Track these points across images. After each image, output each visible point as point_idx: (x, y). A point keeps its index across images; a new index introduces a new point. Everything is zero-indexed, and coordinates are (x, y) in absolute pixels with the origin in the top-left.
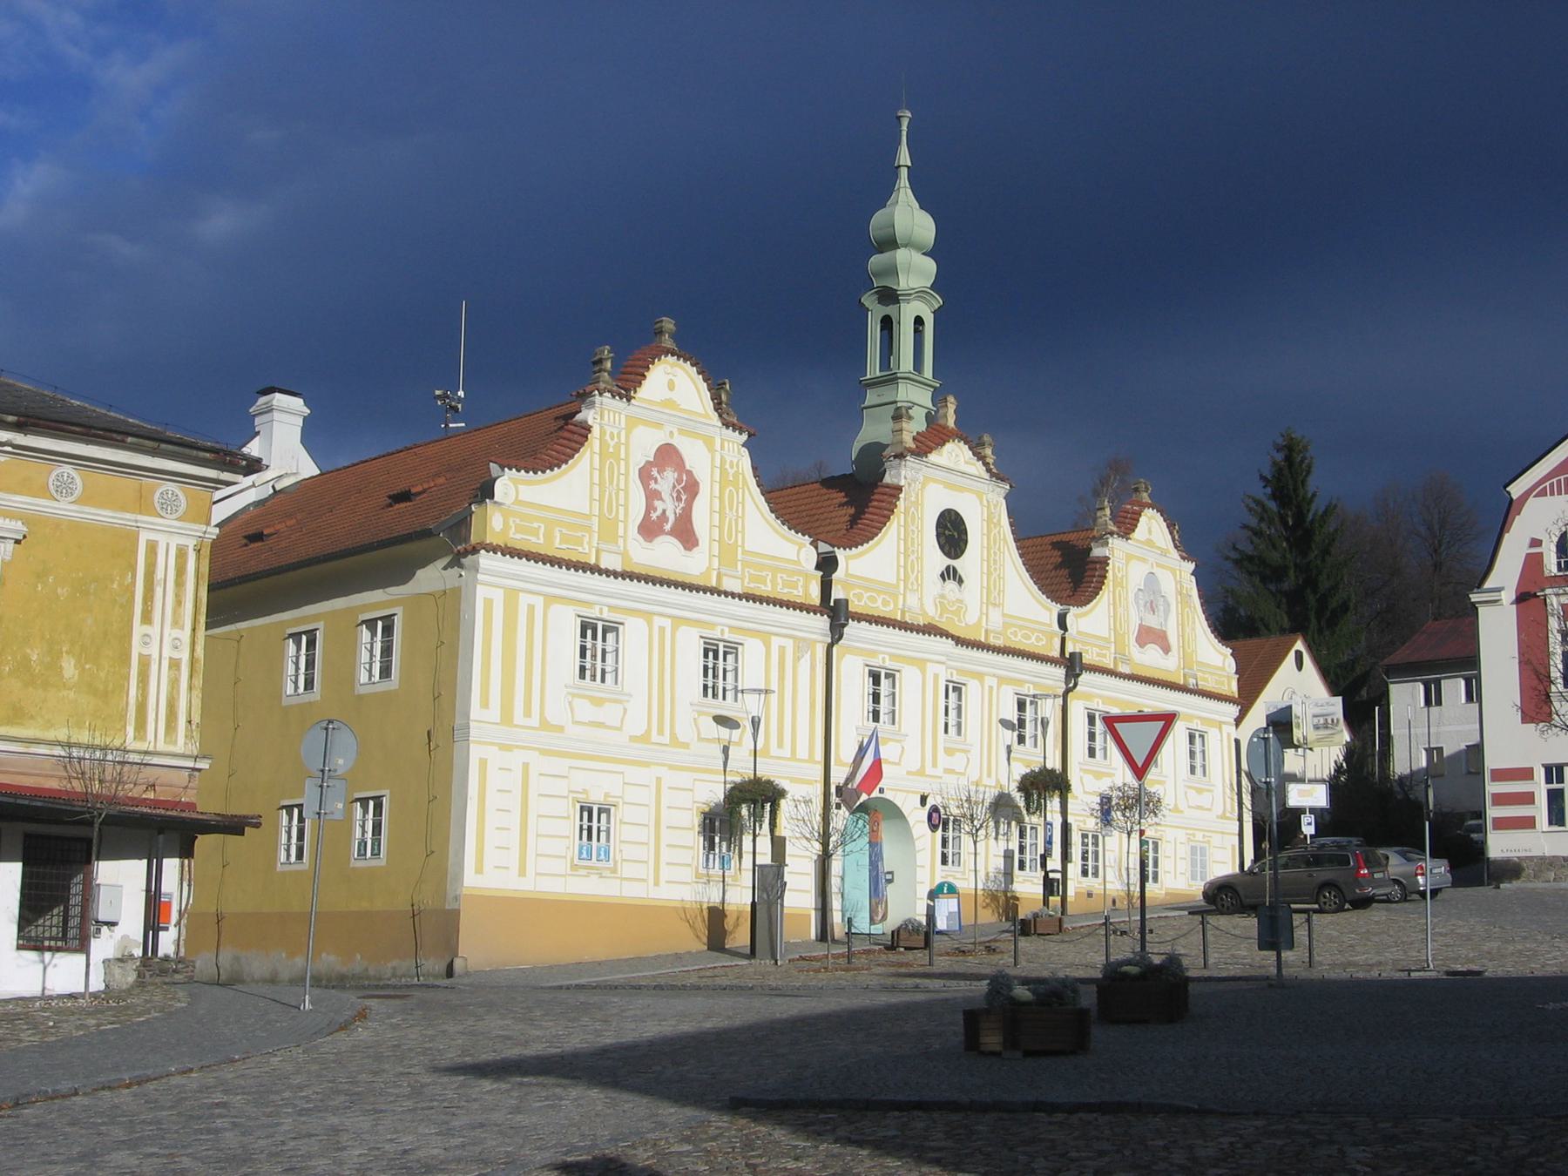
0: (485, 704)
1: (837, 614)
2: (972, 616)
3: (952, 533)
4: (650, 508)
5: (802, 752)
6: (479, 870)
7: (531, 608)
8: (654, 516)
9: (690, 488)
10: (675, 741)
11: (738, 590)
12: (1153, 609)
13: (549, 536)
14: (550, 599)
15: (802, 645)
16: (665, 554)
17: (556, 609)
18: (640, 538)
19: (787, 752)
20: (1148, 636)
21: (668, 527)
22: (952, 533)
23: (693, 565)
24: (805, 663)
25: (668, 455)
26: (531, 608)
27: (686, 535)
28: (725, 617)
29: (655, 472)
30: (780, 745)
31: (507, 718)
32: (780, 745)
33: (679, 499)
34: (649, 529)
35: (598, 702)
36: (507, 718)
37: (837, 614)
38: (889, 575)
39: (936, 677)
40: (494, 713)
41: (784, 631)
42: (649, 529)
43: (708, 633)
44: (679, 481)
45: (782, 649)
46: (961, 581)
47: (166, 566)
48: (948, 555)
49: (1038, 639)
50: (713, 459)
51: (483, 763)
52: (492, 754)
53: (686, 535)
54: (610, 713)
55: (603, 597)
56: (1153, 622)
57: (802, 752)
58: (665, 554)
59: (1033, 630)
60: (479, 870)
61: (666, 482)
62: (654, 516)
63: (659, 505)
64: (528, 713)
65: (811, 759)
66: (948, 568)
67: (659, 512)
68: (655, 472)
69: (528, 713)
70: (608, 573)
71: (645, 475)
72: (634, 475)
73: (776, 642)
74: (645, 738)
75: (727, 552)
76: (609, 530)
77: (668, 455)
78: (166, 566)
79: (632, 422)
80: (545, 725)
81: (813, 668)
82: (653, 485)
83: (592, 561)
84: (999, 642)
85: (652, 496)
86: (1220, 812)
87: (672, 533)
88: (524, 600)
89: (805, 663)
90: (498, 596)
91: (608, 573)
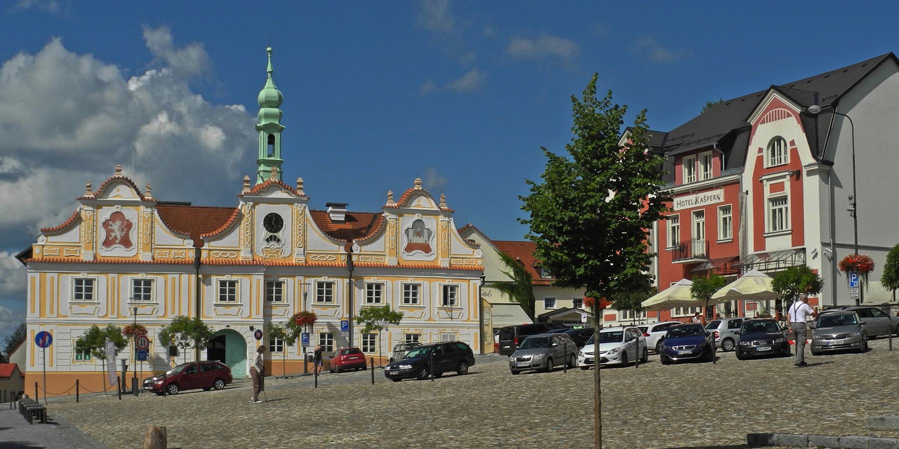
1: (198, 264)
9: (129, 225)
12: (419, 234)
25: (116, 216)
27: (126, 242)
29: (111, 223)
33: (123, 230)
34: (107, 243)
42: (107, 243)
46: (279, 241)
48: (271, 231)
53: (126, 242)
58: (118, 252)
61: (116, 226)
63: (113, 234)
68: (111, 223)
72: (100, 225)
87: (120, 243)
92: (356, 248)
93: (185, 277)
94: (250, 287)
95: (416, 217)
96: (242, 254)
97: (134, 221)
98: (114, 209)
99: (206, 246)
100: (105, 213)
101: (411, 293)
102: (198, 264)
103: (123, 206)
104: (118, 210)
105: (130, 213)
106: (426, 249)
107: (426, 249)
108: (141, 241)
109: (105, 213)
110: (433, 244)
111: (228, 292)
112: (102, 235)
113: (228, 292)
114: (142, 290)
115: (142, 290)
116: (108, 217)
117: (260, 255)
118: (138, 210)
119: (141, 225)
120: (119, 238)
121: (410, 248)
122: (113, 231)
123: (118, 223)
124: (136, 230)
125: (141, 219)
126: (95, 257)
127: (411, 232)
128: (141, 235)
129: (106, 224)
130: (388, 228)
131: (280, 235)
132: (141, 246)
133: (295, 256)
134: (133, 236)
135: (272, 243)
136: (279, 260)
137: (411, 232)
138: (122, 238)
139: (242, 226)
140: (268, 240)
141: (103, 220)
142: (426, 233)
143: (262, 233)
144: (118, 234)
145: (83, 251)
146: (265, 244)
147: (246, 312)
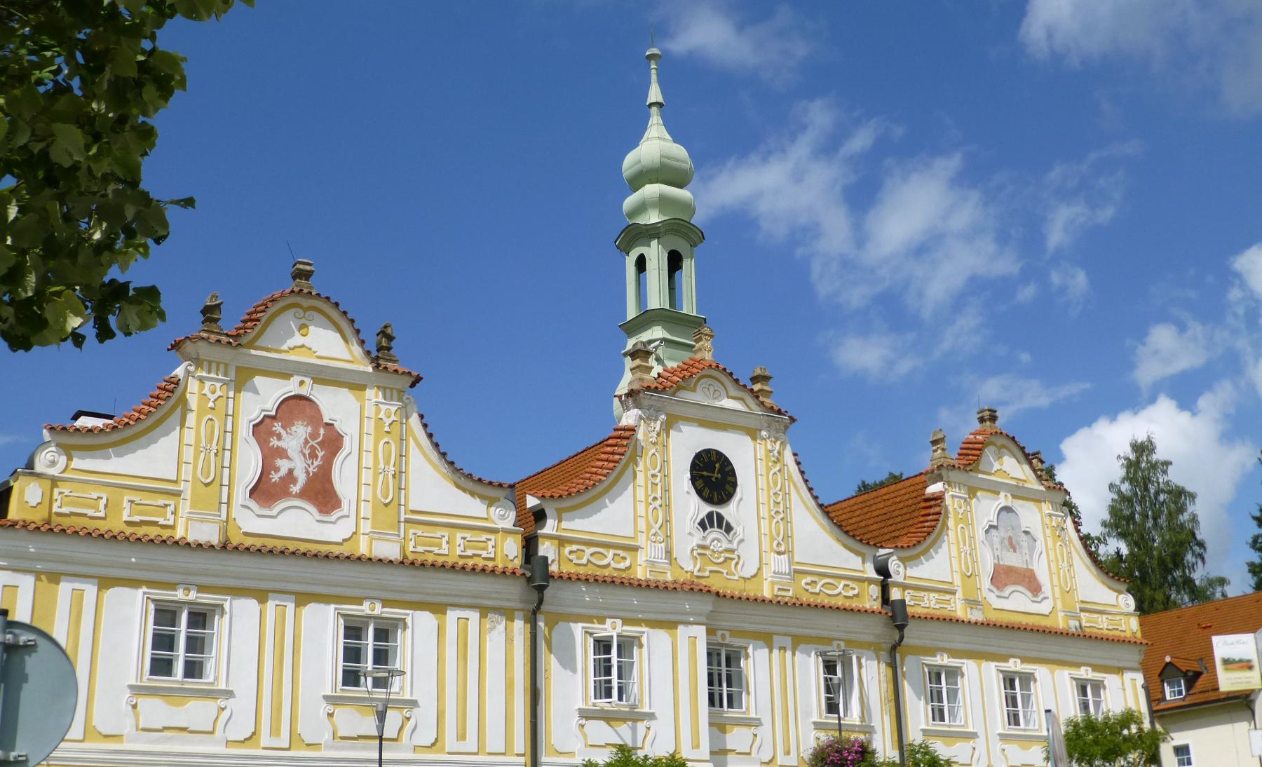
1: (535, 577)
3: (713, 478)
8: (275, 477)
9: (332, 442)
10: (295, 739)
12: (1012, 546)
18: (252, 504)
20: (1003, 577)
21: (296, 489)
22: (713, 478)
25: (296, 406)
27: (322, 494)
29: (278, 427)
33: (313, 456)
34: (265, 491)
41: (464, 601)
42: (265, 491)
44: (314, 436)
46: (729, 529)
48: (708, 500)
50: (362, 409)
53: (322, 494)
54: (196, 712)
56: (1012, 560)
58: (295, 522)
61: (294, 439)
62: (275, 477)
63: (284, 465)
66: (710, 515)
67: (283, 472)
71: (262, 429)
72: (245, 430)
81: (509, 640)
82: (274, 442)
83: (179, 533)
85: (271, 456)
87: (303, 495)
95: (1004, 500)
96: (642, 557)
97: (348, 427)
98: (291, 387)
99: (550, 527)
100: (268, 394)
103: (316, 381)
104: (304, 391)
105: (336, 405)
107: (1030, 582)
108: (366, 493)
109: (268, 394)
112: (249, 463)
116: (271, 406)
117: (689, 566)
118: (361, 400)
119: (368, 443)
120: (302, 478)
122: (282, 453)
123: (301, 430)
124: (354, 458)
125: (369, 426)
126: (224, 530)
128: (367, 476)
129: (262, 429)
130: (951, 523)
131: (728, 512)
132: (366, 510)
133: (767, 573)
134: (344, 478)
135: (714, 533)
139: (641, 478)
140: (702, 524)
144: (297, 465)
145: (185, 508)
146: (698, 537)
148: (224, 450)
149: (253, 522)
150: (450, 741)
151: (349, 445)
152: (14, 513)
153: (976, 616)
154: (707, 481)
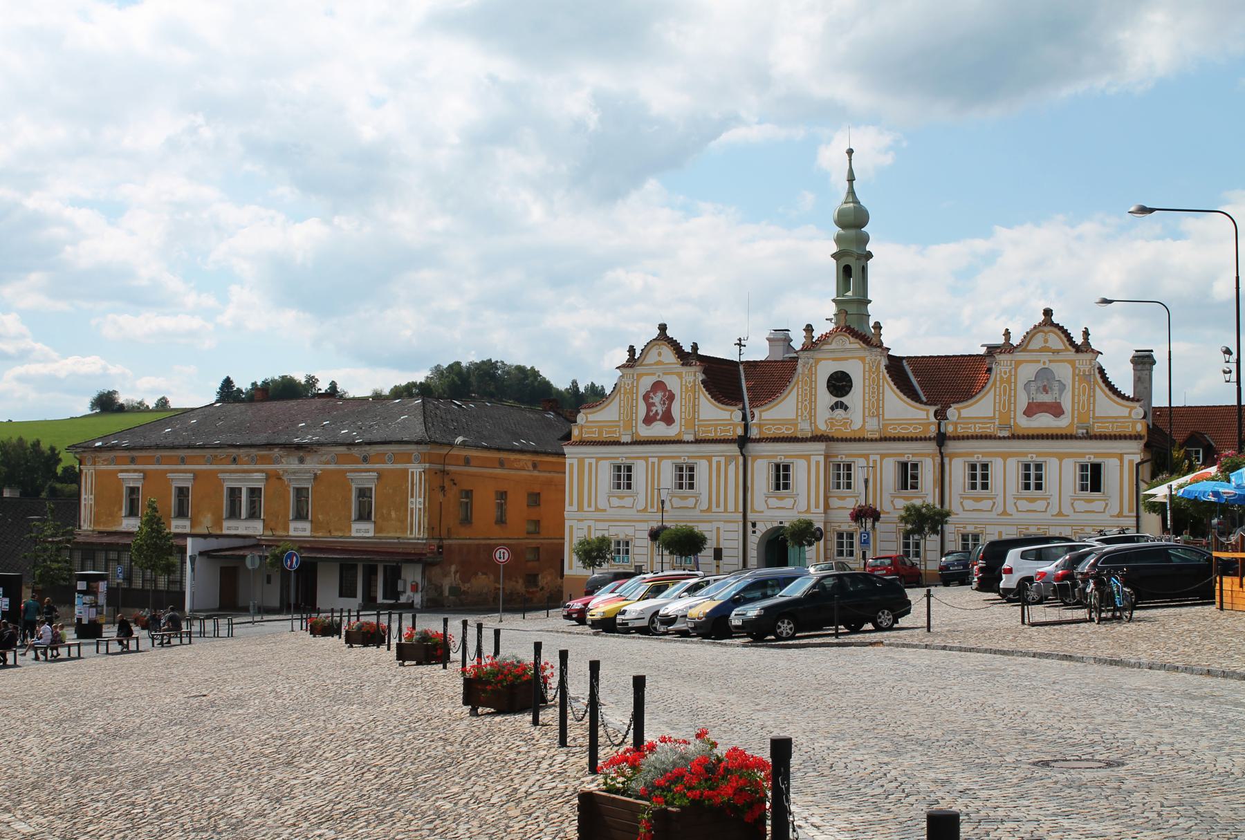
0: (571, 504)
2: (857, 424)
3: (840, 384)
4: (649, 410)
5: (731, 507)
6: (570, 568)
7: (590, 464)
9: (671, 397)
11: (690, 438)
12: (1045, 390)
13: (600, 433)
14: (598, 459)
15: (729, 459)
16: (659, 429)
17: (601, 463)
19: (722, 509)
22: (840, 384)
23: (671, 432)
24: (732, 467)
25: (658, 386)
26: (590, 464)
27: (668, 419)
28: (684, 453)
30: (718, 506)
31: (580, 508)
32: (718, 506)
34: (648, 420)
35: (619, 497)
36: (580, 508)
37: (743, 441)
38: (791, 415)
39: (818, 463)
40: (575, 508)
42: (648, 420)
43: (677, 461)
45: (718, 463)
46: (846, 408)
47: (416, 478)
48: (836, 396)
49: (915, 428)
51: (571, 527)
52: (574, 523)
53: (668, 419)
54: (628, 502)
55: (621, 454)
57: (731, 507)
58: (659, 429)
59: (910, 425)
60: (570, 568)
61: (657, 398)
63: (654, 409)
64: (589, 505)
65: (736, 511)
66: (836, 403)
69: (589, 505)
70: (623, 444)
71: (646, 397)
73: (715, 460)
74: (645, 510)
75: (692, 421)
76: (630, 423)
77: (658, 386)
78: (416, 478)
79: (640, 376)
80: (597, 509)
81: (737, 468)
84: (877, 436)
85: (649, 406)
86: (1116, 512)
87: (662, 419)
88: (587, 461)
89: (732, 467)
90: (575, 462)
91: (623, 444)
92: (952, 412)
93: (729, 459)
94: (808, 469)
101: (1033, 478)
102: (743, 441)
105: (673, 384)
106: (1056, 410)
107: (1056, 410)
109: (646, 383)
110: (1067, 405)
111: (782, 478)
112: (642, 410)
113: (782, 478)
114: (685, 477)
115: (685, 477)
117: (822, 427)
120: (660, 412)
121: (1030, 411)
122: (653, 404)
123: (660, 394)
127: (1033, 387)
129: (646, 397)
135: (839, 411)
136: (847, 432)
137: (1033, 387)
138: (664, 413)
140: (832, 408)
141: (642, 391)
142: (1056, 386)
143: (825, 398)
144: (659, 408)
147: (802, 505)
148: (633, 408)
149: (645, 432)
150: (714, 508)
151: (677, 397)
152: (573, 439)
153: (1006, 434)
154: (834, 385)
